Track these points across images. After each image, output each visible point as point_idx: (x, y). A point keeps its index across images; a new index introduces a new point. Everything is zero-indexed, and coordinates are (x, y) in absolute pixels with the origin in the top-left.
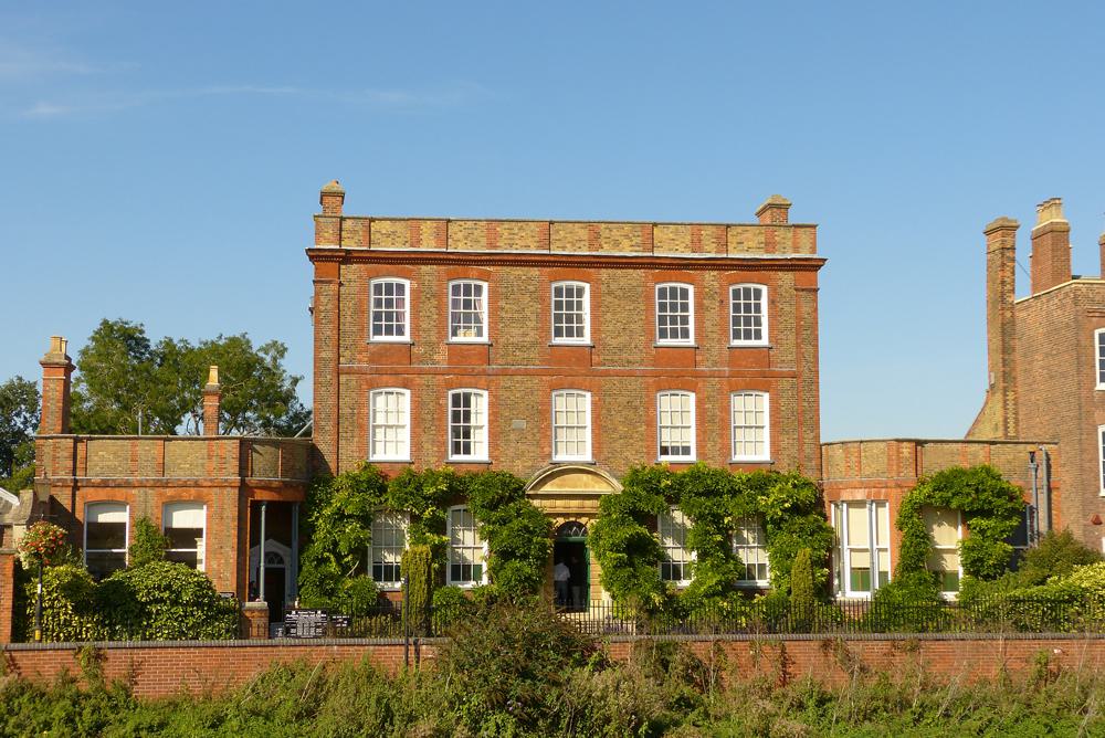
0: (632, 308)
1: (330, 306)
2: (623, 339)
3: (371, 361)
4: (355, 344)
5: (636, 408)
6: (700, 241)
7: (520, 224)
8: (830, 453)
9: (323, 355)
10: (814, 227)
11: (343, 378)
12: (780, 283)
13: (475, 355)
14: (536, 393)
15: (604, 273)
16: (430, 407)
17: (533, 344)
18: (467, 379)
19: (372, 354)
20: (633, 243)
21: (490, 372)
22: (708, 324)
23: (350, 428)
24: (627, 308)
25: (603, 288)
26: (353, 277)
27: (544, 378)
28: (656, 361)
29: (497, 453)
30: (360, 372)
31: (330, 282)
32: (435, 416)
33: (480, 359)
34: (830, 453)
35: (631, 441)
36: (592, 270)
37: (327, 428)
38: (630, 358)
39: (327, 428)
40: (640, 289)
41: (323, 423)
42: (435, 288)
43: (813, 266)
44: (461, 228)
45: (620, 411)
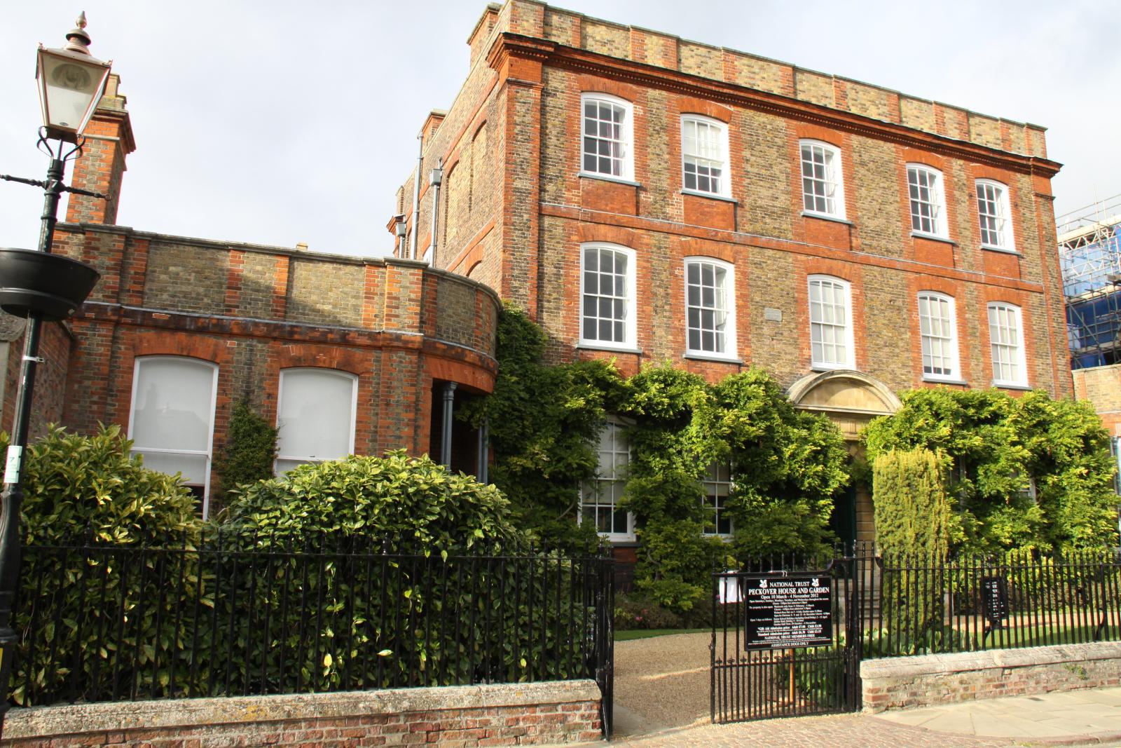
0: (886, 185)
1: (528, 119)
2: (880, 222)
3: (585, 202)
4: (560, 175)
5: (899, 309)
6: (944, 123)
7: (761, 63)
8: (1088, 382)
9: (518, 184)
10: (1042, 130)
11: (547, 221)
12: (1019, 186)
13: (718, 214)
14: (790, 275)
15: (856, 140)
16: (663, 277)
17: (785, 212)
18: (708, 246)
19: (587, 193)
20: (880, 111)
21: (737, 239)
22: (960, 219)
23: (555, 295)
24: (882, 185)
25: (855, 156)
26: (561, 86)
27: (799, 257)
28: (914, 254)
29: (747, 351)
30: (567, 217)
31: (530, 86)
32: (670, 291)
33: (724, 220)
34: (1088, 382)
35: (897, 350)
36: (843, 134)
37: (522, 291)
38: (890, 246)
39: (522, 291)
40: (893, 166)
41: (516, 284)
42: (665, 120)
43: (1047, 169)
44: (693, 53)
45: (882, 311)
